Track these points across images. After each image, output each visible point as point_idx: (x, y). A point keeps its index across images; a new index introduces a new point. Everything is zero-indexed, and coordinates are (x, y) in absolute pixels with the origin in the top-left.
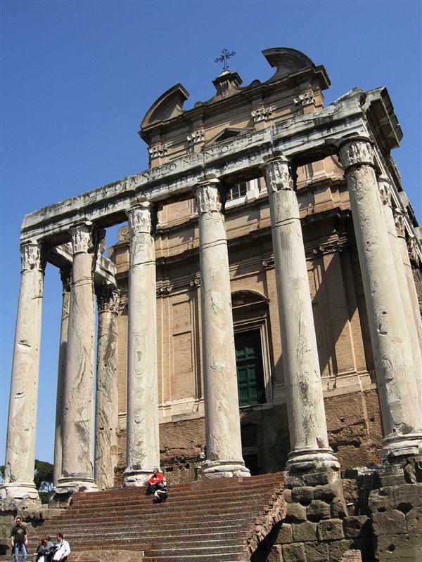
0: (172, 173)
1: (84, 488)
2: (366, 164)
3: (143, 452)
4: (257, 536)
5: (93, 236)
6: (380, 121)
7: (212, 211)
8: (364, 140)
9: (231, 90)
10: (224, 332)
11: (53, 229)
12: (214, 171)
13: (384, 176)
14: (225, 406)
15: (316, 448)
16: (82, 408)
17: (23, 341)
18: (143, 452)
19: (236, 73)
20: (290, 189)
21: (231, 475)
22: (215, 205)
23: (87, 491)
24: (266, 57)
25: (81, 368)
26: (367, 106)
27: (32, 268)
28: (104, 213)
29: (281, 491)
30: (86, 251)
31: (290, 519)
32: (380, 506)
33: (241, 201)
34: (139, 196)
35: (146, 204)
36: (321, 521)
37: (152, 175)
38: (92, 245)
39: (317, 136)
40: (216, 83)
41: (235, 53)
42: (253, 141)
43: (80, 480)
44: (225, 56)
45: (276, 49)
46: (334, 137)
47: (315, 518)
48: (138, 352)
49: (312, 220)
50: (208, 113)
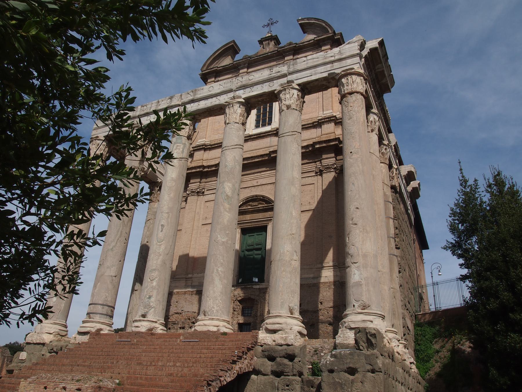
1: (101, 330)
2: (357, 92)
4: (220, 381)
6: (376, 68)
8: (359, 74)
9: (271, 47)
10: (229, 215)
13: (375, 110)
19: (276, 36)
20: (296, 110)
22: (238, 118)
23: (102, 332)
24: (301, 25)
26: (365, 53)
29: (252, 347)
31: (257, 372)
32: (330, 368)
33: (267, 128)
36: (282, 377)
40: (261, 42)
41: (278, 22)
42: (274, 72)
44: (271, 24)
45: (308, 19)
46: (337, 71)
47: (277, 374)
48: (162, 226)
49: (317, 146)
50: (252, 63)
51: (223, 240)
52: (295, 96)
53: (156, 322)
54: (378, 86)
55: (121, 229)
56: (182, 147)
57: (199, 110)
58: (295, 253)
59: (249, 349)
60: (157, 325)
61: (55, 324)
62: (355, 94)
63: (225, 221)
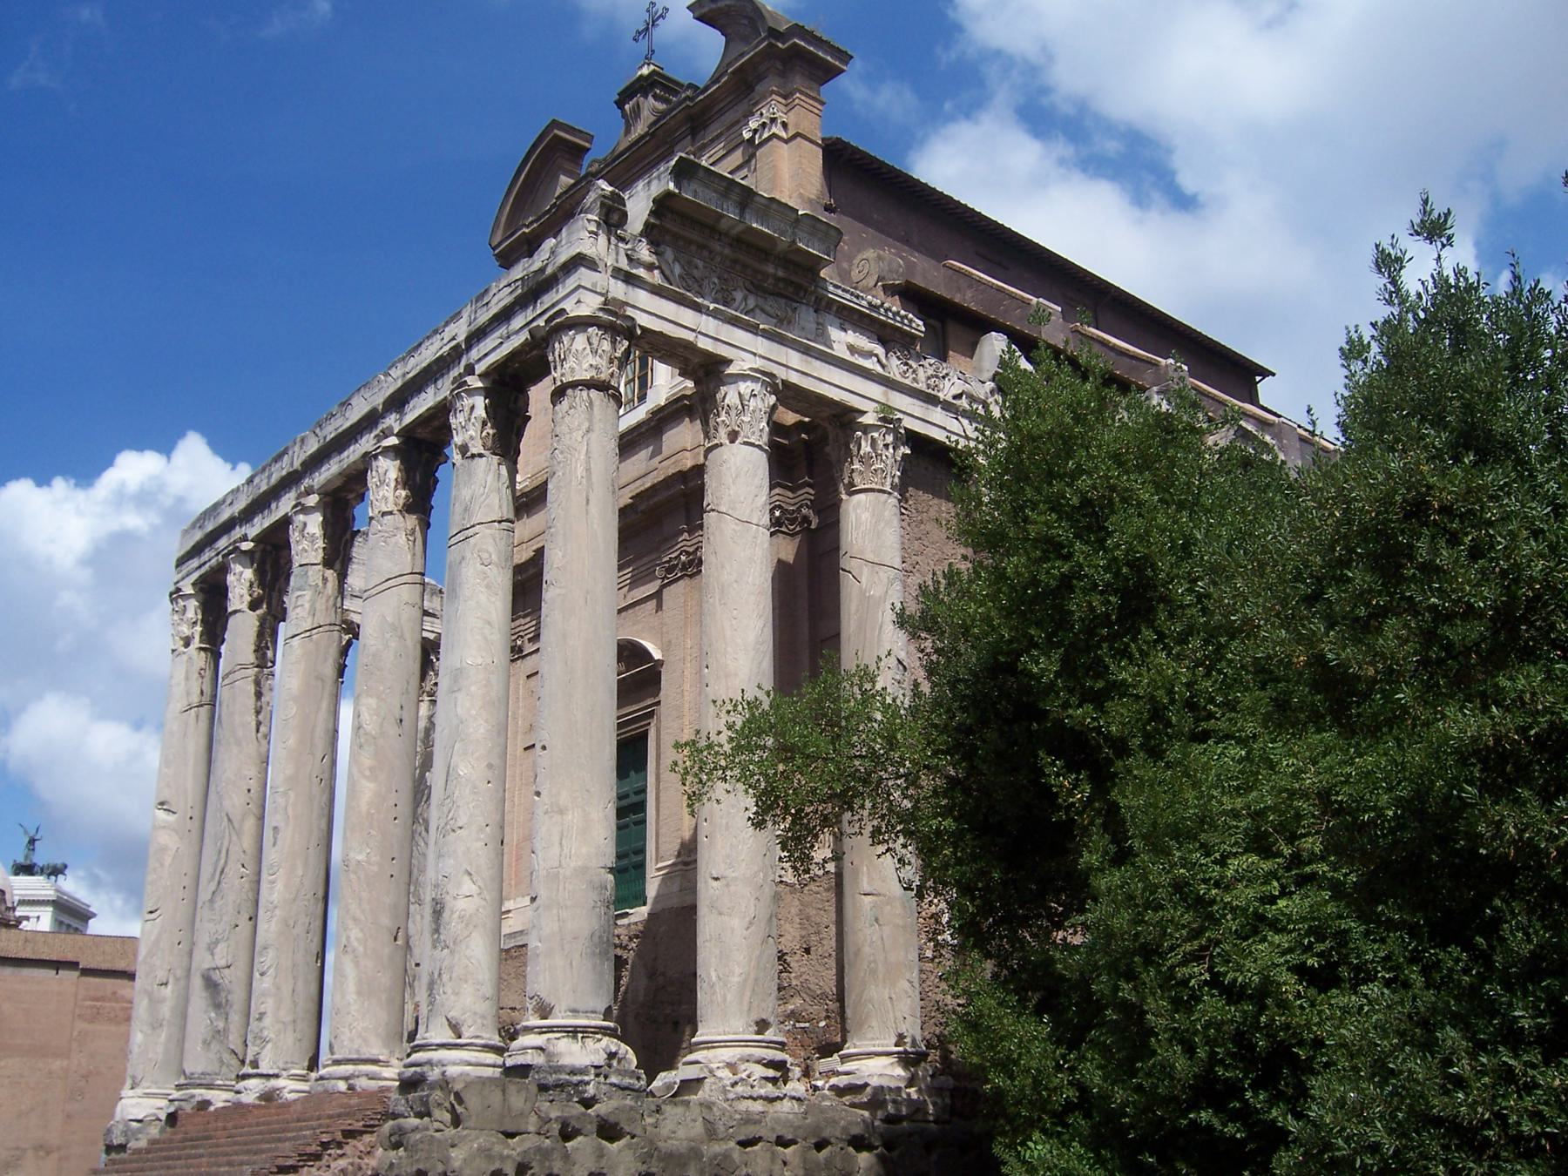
0: (347, 424)
2: (574, 385)
3: (266, 1033)
5: (260, 573)
7: (384, 514)
10: (372, 785)
11: (210, 558)
12: (394, 416)
14: (355, 944)
15: (447, 1036)
16: (217, 942)
17: (162, 803)
18: (266, 1033)
20: (481, 456)
21: (342, 1086)
22: (391, 499)
25: (218, 860)
27: (187, 645)
28: (266, 525)
30: (244, 607)
34: (306, 482)
35: (312, 500)
37: (325, 432)
38: (258, 591)
39: (518, 322)
43: (200, 1086)
48: (275, 828)
51: (360, 858)
52: (481, 412)
53: (277, 1076)
54: (771, 269)
55: (226, 844)
56: (308, 598)
57: (329, 481)
58: (466, 878)
59: (350, 1134)
60: (280, 1083)
61: (147, 1095)
62: (569, 392)
63: (364, 808)
